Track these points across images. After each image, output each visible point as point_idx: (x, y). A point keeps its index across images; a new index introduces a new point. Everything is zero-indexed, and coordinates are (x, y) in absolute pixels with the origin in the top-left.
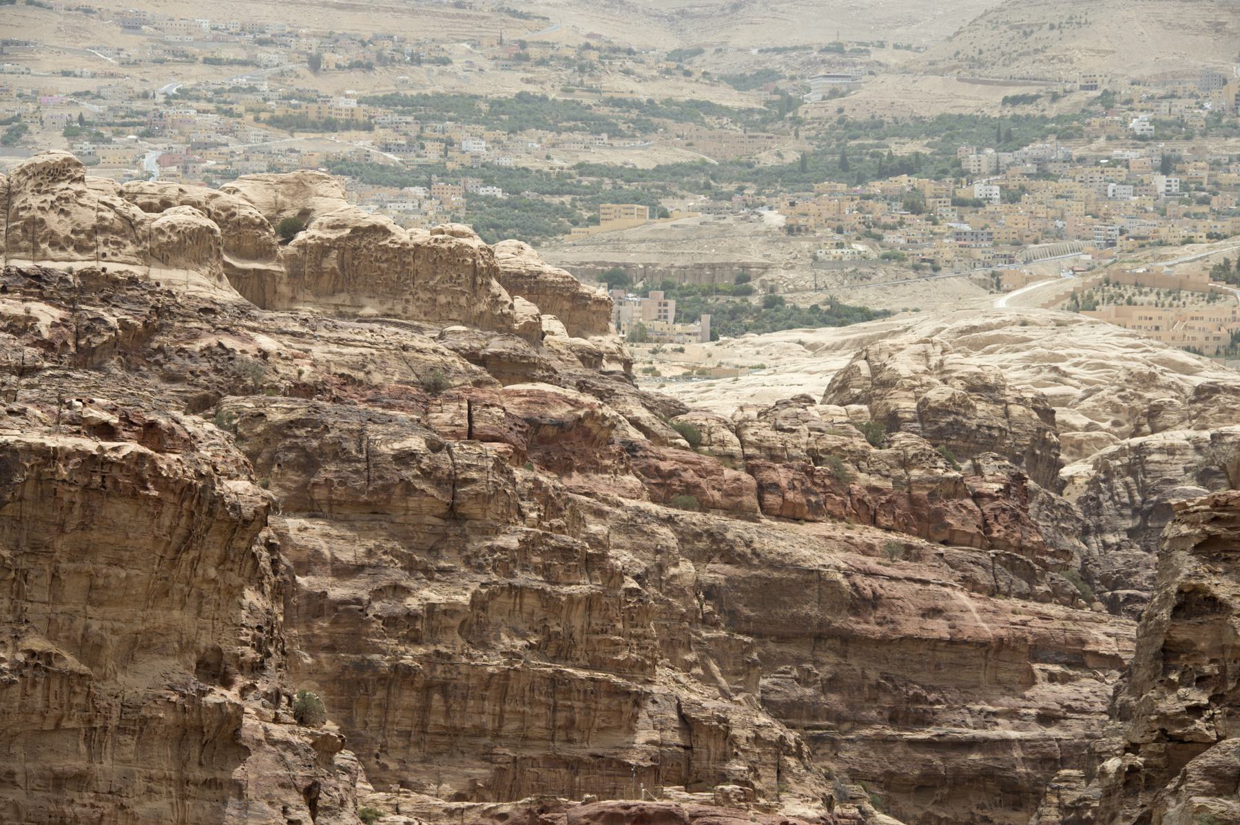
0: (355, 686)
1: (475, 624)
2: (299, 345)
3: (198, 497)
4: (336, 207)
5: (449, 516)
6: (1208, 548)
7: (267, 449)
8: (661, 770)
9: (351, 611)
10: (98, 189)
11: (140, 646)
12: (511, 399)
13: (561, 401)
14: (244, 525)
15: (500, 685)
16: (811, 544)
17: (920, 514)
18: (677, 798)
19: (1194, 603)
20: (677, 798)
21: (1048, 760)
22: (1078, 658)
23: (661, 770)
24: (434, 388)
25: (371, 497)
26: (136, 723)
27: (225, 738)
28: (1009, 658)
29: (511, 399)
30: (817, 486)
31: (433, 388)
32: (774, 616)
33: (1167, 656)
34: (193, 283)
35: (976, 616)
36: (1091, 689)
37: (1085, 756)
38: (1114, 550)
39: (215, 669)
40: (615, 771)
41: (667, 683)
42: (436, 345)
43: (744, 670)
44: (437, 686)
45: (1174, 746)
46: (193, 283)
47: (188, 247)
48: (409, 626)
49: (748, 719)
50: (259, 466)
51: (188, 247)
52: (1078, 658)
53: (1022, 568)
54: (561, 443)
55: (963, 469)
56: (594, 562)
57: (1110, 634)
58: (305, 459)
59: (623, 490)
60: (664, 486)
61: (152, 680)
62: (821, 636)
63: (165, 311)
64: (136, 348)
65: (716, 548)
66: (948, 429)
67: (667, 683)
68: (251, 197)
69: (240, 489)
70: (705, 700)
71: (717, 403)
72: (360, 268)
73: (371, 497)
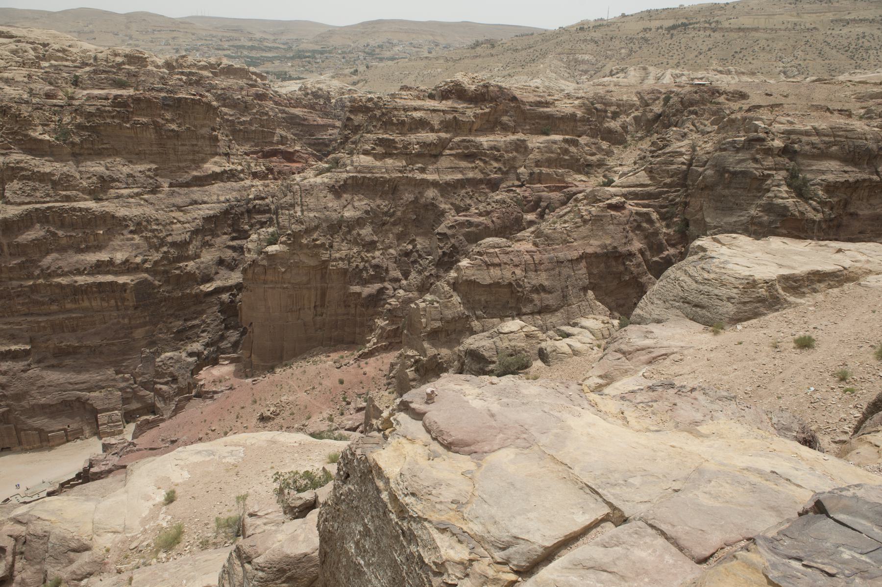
0: (235, 133)
1: (250, 123)
2: (222, 82)
3: (209, 105)
4: (225, 62)
5: (245, 108)
6: (350, 112)
7: (218, 98)
8: (278, 143)
9: (232, 121)
10: (190, 59)
11: (202, 126)
12: (253, 90)
13: (261, 91)
14: (216, 109)
15: (255, 131)
16: (297, 111)
17: (312, 107)
18: (281, 147)
19: (349, 119)
20: (281, 147)
21: (331, 141)
22: (334, 127)
23: (278, 143)
24: (242, 89)
25: (234, 104)
26: (203, 137)
27: (216, 139)
28: (325, 127)
29: (253, 90)
30: (298, 103)
31: (242, 89)
32: (292, 122)
33: (345, 126)
34: (205, 73)
35: (320, 121)
36: (336, 131)
37: (335, 140)
38: (338, 112)
39: (214, 129)
40: (272, 143)
41: (278, 131)
42: (242, 82)
43: (289, 129)
44: (246, 131)
45: (346, 139)
46: (205, 73)
47: (204, 68)
48: (241, 123)
49: (290, 136)
50: (217, 100)
51: (204, 68)
52: (334, 127)
53: (326, 115)
54: (261, 97)
55: (317, 100)
56: (267, 114)
57: (338, 124)
58: (223, 99)
59: (270, 104)
60: (276, 103)
61: (205, 131)
62: (299, 124)
63: (201, 77)
64: (198, 83)
65: (284, 112)
66: (315, 95)
67: (278, 131)
68: (213, 60)
69: (215, 103)
70: (284, 133)
71: (283, 91)
72: (229, 71)
73: (234, 104)
